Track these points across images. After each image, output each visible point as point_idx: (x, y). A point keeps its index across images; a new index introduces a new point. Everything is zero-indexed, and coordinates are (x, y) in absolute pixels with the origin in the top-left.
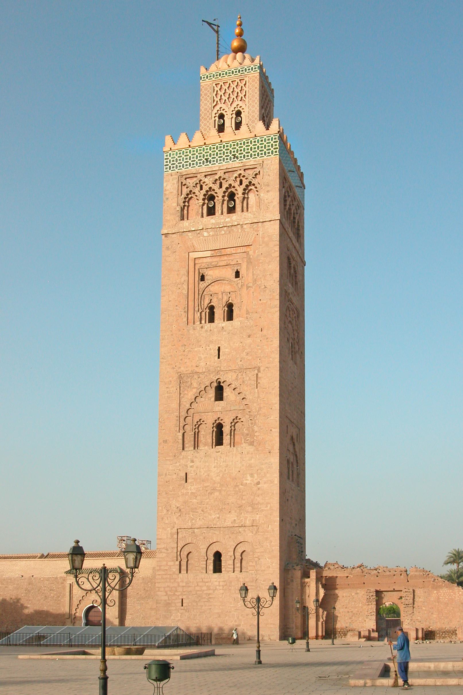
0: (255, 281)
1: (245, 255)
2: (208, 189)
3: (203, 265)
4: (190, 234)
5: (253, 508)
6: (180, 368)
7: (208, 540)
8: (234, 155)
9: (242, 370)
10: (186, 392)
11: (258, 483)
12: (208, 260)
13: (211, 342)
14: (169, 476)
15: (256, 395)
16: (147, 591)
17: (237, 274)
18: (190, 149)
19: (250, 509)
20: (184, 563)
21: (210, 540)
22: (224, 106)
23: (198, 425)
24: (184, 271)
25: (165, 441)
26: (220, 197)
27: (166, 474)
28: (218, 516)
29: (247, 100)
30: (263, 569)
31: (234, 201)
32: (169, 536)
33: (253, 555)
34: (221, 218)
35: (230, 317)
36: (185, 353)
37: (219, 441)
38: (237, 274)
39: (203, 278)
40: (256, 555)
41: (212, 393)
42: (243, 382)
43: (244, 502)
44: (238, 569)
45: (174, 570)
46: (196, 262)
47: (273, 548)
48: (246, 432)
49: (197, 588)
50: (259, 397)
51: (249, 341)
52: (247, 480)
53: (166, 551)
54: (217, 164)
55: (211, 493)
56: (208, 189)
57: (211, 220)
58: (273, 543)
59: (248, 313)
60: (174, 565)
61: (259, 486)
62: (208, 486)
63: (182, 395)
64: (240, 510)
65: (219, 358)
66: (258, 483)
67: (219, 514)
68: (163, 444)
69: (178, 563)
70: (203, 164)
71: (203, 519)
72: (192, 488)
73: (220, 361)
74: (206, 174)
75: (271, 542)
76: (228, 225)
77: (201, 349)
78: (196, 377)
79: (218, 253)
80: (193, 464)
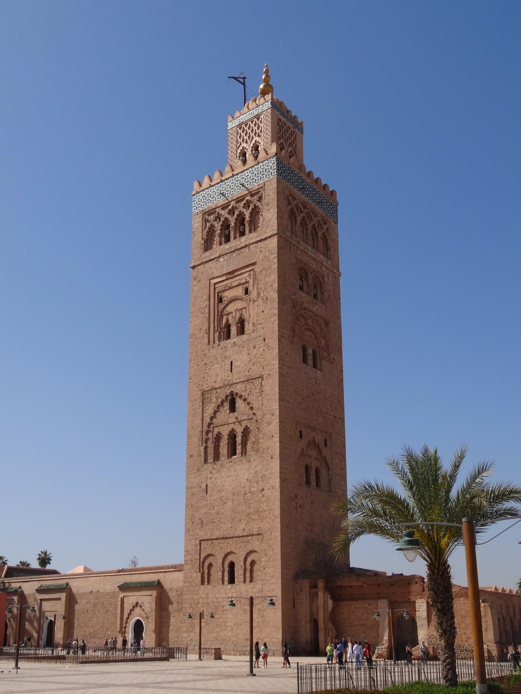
0: (259, 294)
1: (252, 273)
2: (224, 219)
3: (221, 288)
5: (259, 516)
6: (202, 385)
10: (207, 407)
11: (263, 490)
12: (225, 283)
13: (226, 357)
14: (194, 489)
15: (261, 403)
16: (179, 603)
17: (247, 291)
19: (255, 517)
20: (206, 575)
22: (245, 145)
23: (219, 437)
24: (206, 297)
25: (191, 456)
26: (233, 224)
27: (192, 488)
28: (231, 525)
30: (267, 578)
31: (244, 225)
32: (193, 548)
33: (260, 563)
34: (234, 243)
35: (241, 331)
36: (207, 371)
37: (233, 452)
38: (247, 291)
39: (220, 300)
40: (262, 565)
41: (227, 405)
42: (251, 391)
43: (251, 510)
44: (248, 579)
45: (197, 582)
46: (216, 287)
48: (254, 440)
49: (215, 600)
50: (263, 404)
51: (255, 351)
52: (254, 487)
55: (225, 503)
56: (224, 219)
57: (226, 247)
58: (275, 551)
59: (254, 325)
60: (197, 576)
61: (263, 492)
63: (204, 411)
64: (248, 519)
65: (231, 371)
66: (263, 490)
69: (200, 574)
73: (233, 375)
75: (274, 550)
76: (238, 248)
77: (218, 365)
79: (231, 274)
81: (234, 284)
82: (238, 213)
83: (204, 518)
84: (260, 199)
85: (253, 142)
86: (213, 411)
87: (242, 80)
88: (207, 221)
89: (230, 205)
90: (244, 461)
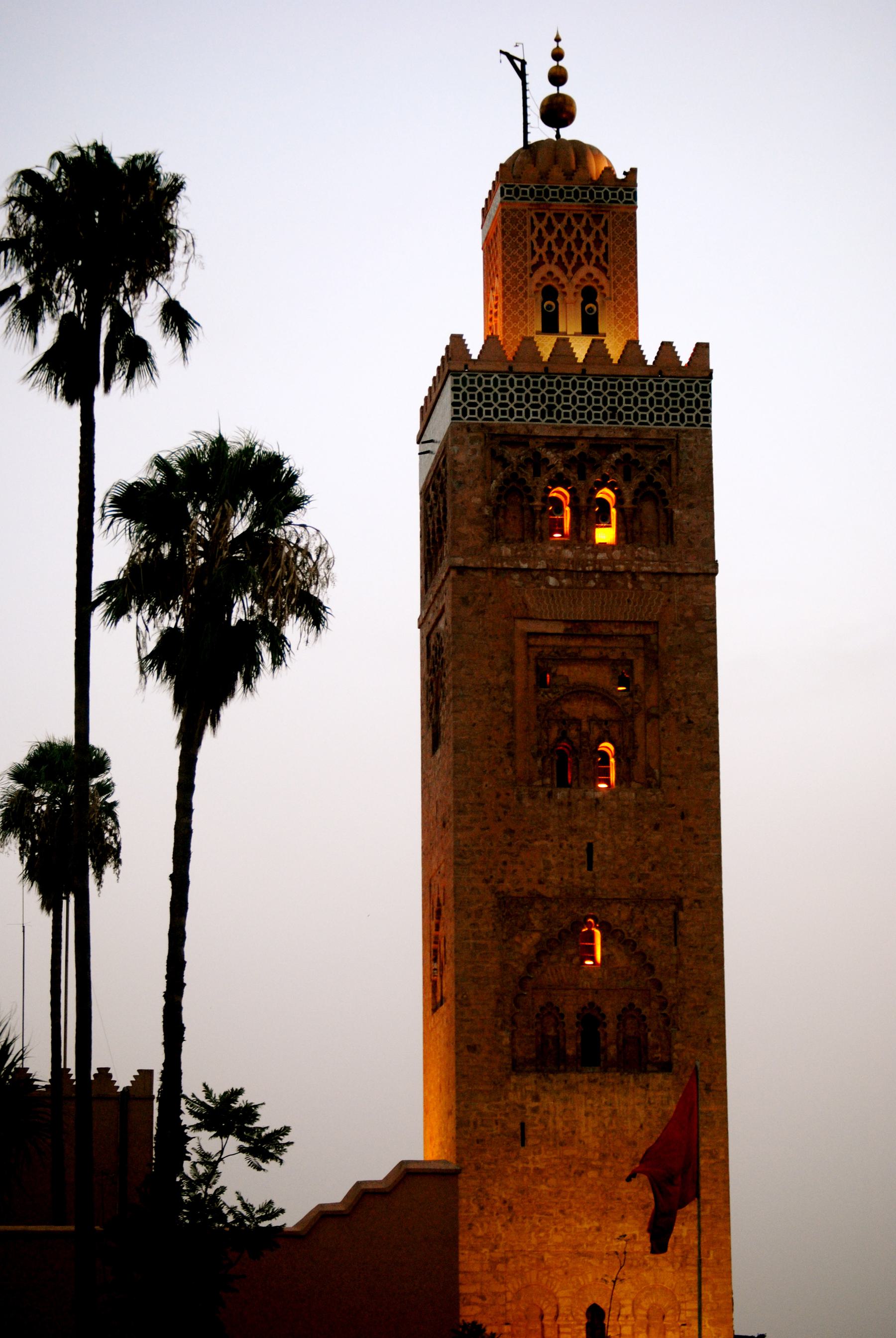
4: (516, 576)
7: (574, 1279)
8: (613, 409)
9: (640, 901)
10: (517, 939)
12: (559, 642)
13: (573, 830)
14: (482, 1129)
18: (511, 376)
21: (580, 1279)
25: (472, 1048)
28: (596, 1224)
29: (610, 267)
32: (486, 1267)
47: (721, 1302)
51: (657, 837)
53: (479, 1301)
54: (574, 423)
55: (580, 1174)
62: (573, 1156)
65: (590, 868)
67: (599, 1220)
68: (466, 1053)
70: (543, 417)
71: (563, 1230)
72: (537, 1158)
74: (549, 441)
76: (604, 568)
77: (549, 844)
78: (538, 906)
79: (579, 628)
80: (537, 1104)
81: (586, 653)
83: (515, 1200)
86: (533, 952)
87: (518, 64)
89: (572, 447)
90: (632, 1084)
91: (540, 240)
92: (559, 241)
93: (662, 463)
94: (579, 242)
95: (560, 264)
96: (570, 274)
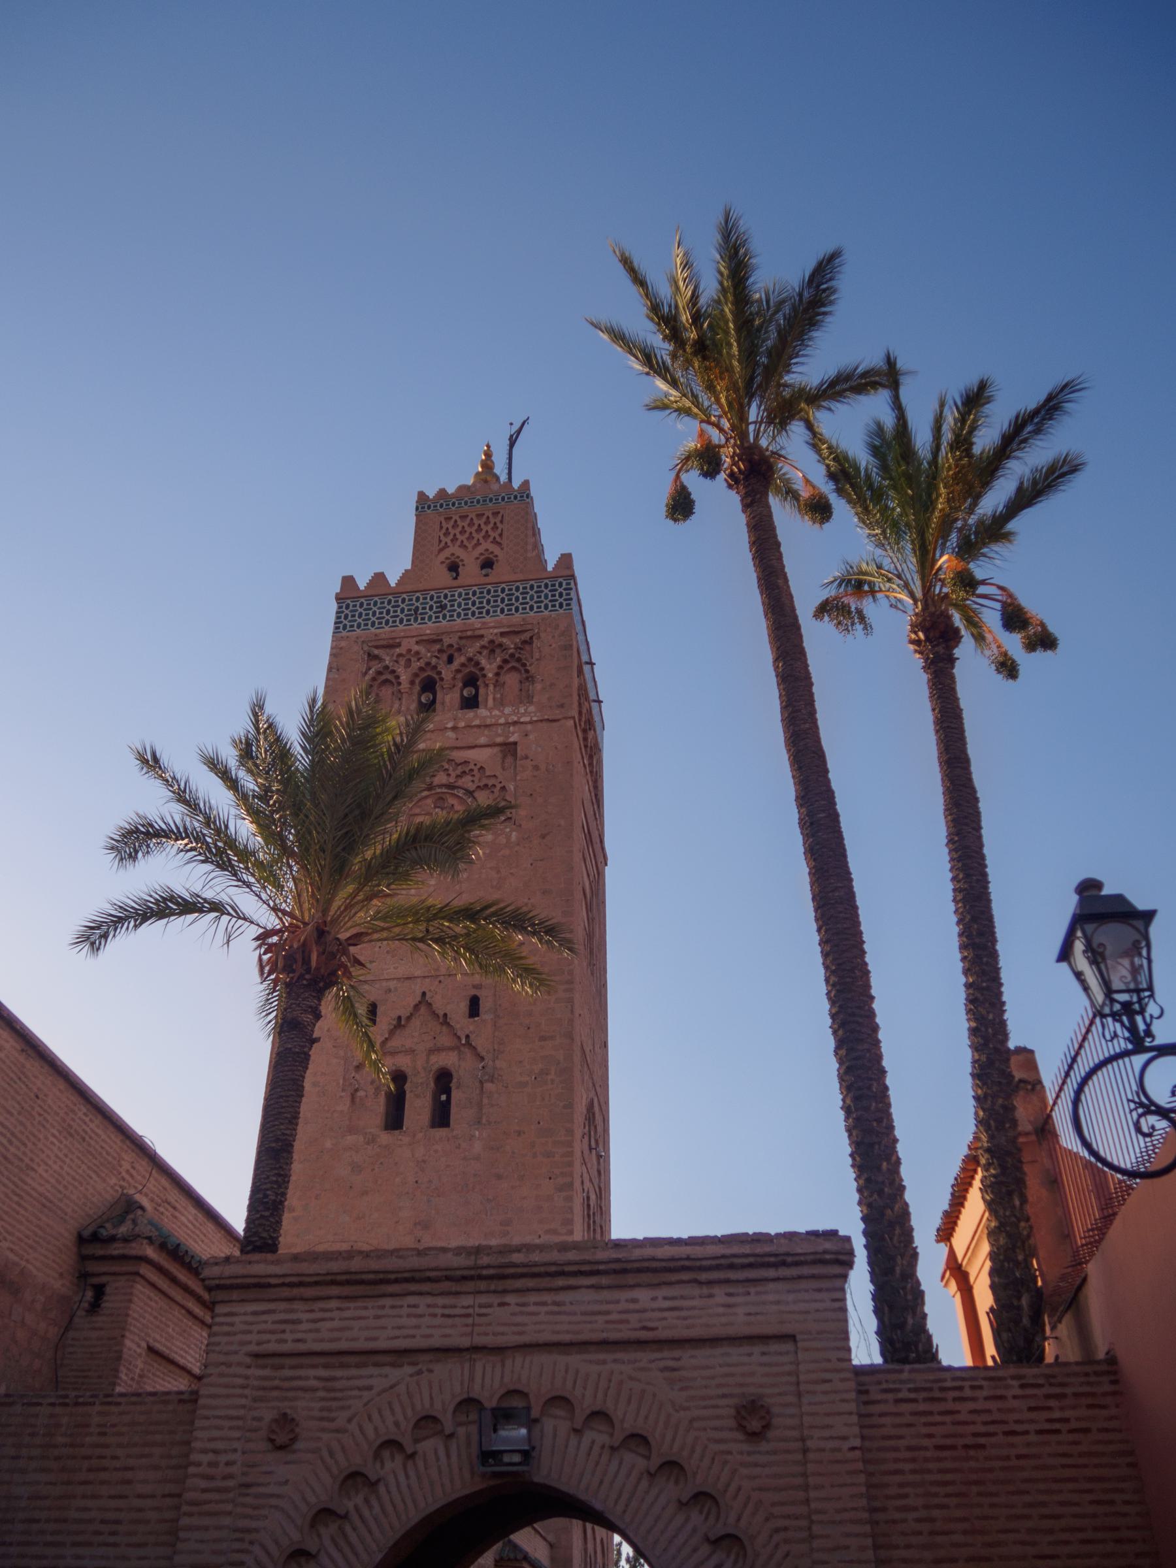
29: (504, 542)
82: (463, 659)
84: (529, 642)
85: (480, 549)
88: (372, 657)
91: (447, 534)
92: (463, 532)
93: (525, 642)
94: (479, 529)
95: (462, 546)
96: (470, 549)
